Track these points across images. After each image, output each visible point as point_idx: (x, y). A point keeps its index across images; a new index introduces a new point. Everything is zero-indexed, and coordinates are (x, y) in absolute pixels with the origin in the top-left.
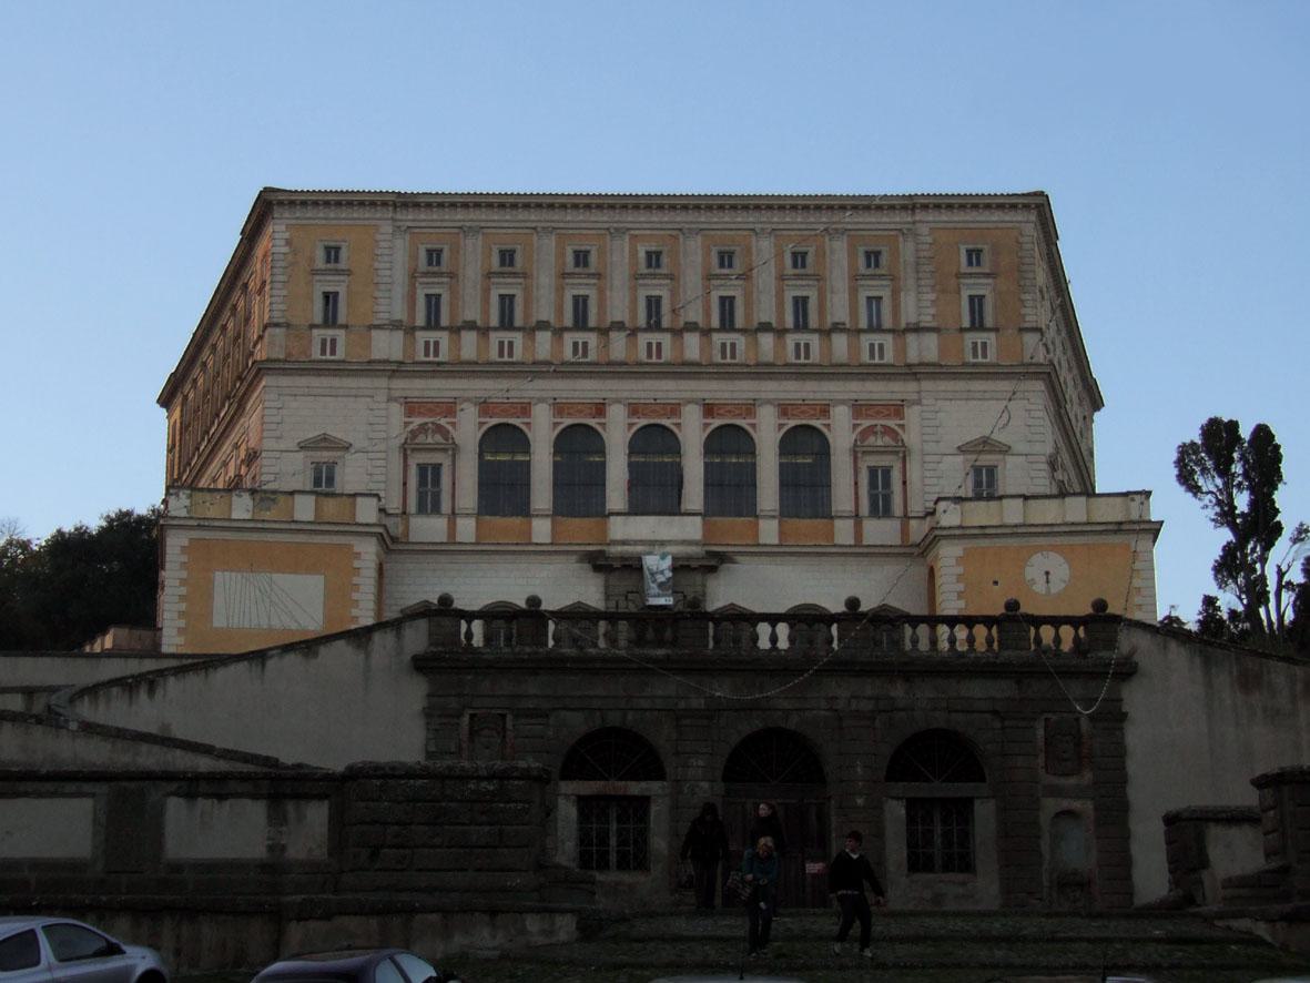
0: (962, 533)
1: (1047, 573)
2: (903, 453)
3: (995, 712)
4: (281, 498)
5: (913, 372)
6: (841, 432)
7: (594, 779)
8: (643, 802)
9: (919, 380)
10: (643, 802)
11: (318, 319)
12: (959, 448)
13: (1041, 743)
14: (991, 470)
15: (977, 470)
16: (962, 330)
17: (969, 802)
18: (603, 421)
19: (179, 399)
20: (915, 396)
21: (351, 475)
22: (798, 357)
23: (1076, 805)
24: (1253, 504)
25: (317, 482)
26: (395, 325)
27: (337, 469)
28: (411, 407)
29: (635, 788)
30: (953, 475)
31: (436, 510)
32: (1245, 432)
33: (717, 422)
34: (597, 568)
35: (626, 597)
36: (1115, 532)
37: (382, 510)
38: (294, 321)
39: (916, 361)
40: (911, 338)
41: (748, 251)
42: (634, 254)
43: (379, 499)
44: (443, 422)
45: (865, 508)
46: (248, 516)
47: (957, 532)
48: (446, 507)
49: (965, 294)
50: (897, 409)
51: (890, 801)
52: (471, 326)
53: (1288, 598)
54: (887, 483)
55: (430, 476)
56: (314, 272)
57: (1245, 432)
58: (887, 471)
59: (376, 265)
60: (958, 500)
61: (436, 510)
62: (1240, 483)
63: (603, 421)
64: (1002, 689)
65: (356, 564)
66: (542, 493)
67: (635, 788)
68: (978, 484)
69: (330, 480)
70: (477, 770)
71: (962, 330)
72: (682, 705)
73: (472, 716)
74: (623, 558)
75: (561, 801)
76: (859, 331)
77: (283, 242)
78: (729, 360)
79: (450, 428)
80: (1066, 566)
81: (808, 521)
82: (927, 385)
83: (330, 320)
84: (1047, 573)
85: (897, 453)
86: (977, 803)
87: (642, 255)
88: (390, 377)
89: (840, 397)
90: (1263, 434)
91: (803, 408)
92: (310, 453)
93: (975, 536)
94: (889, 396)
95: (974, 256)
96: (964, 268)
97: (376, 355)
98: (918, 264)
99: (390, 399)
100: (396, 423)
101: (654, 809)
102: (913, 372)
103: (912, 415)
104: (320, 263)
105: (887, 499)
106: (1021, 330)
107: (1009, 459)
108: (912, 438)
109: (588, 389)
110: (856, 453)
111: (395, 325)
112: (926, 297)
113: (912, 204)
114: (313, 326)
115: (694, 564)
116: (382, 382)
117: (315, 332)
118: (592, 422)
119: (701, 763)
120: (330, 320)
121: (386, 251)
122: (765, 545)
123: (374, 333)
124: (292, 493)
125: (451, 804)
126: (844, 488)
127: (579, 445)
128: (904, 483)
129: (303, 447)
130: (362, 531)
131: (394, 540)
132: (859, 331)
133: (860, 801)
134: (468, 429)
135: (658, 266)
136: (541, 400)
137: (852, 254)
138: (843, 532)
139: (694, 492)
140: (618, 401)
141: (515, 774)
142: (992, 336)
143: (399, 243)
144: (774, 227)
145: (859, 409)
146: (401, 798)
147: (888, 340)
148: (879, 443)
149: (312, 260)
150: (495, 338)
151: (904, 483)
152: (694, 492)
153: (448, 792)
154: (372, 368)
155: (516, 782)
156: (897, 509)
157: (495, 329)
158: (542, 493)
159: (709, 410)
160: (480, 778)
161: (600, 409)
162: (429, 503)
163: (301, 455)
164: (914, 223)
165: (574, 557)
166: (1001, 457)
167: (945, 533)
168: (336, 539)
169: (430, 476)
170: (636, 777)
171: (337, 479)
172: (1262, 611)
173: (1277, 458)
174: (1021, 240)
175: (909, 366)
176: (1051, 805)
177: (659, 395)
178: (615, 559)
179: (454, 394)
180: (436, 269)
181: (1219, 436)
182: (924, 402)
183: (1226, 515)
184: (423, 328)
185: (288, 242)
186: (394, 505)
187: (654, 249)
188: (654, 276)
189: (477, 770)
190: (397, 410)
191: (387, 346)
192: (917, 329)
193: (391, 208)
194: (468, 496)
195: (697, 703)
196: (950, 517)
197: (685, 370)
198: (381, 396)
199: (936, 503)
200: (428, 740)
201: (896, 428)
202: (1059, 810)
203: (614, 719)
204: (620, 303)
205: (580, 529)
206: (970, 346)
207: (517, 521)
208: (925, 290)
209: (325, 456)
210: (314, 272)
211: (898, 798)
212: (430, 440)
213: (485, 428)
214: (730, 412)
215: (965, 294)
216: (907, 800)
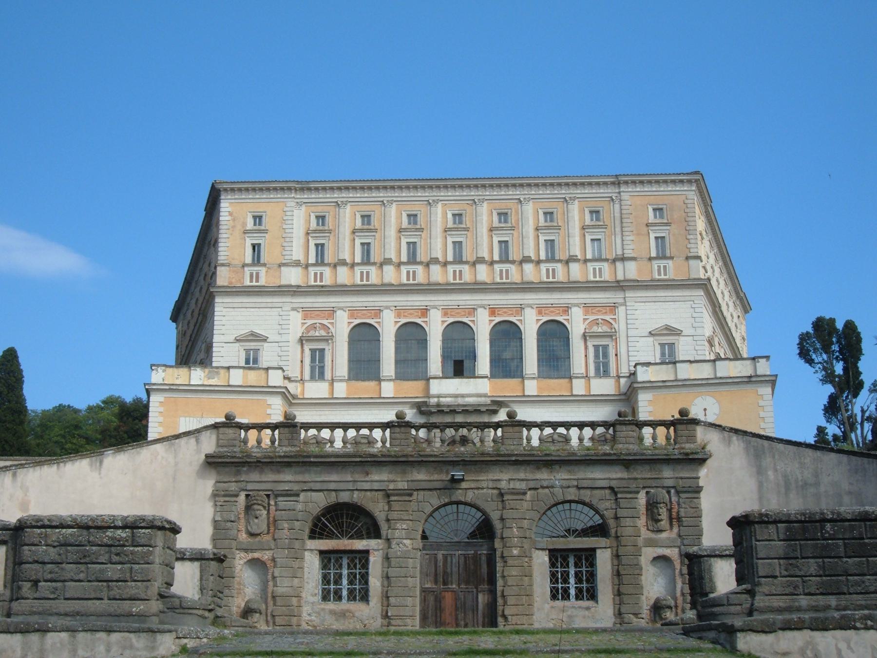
0: (651, 386)
1: (705, 410)
2: (612, 335)
3: (611, 488)
4: (222, 371)
5: (620, 286)
6: (577, 324)
7: (331, 538)
8: (365, 554)
10: (365, 554)
11: (249, 260)
13: (642, 509)
14: (672, 345)
15: (662, 345)
16: (650, 259)
17: (594, 550)
18: (425, 320)
19: (181, 316)
20: (621, 301)
21: (268, 356)
22: (548, 277)
23: (667, 552)
24: (845, 369)
25: (247, 361)
26: (297, 264)
27: (260, 353)
28: (307, 313)
29: (360, 544)
30: (648, 350)
31: (322, 376)
32: (840, 325)
33: (498, 319)
36: (747, 382)
37: (285, 378)
38: (233, 262)
39: (622, 279)
40: (619, 265)
41: (517, 213)
42: (445, 215)
43: (284, 371)
44: (325, 322)
45: (592, 372)
46: (200, 383)
47: (648, 385)
48: (328, 375)
49: (652, 236)
50: (613, 308)
51: (537, 551)
52: (343, 263)
53: (868, 426)
54: (606, 355)
55: (318, 356)
56: (246, 232)
57: (840, 325)
58: (605, 347)
59: (285, 227)
60: (648, 364)
61: (322, 376)
62: (837, 357)
63: (425, 320)
64: (616, 474)
66: (388, 366)
67: (360, 544)
68: (663, 354)
69: (256, 361)
70: (113, 522)
71: (650, 259)
72: (391, 486)
73: (247, 496)
75: (307, 554)
76: (586, 261)
77: (227, 214)
78: (504, 280)
79: (329, 326)
80: (717, 405)
81: (556, 381)
82: (629, 294)
83: (257, 260)
84: (705, 410)
85: (611, 336)
86: (598, 552)
87: (450, 216)
89: (576, 301)
90: (850, 326)
91: (552, 309)
92: (242, 344)
93: (660, 387)
94: (605, 301)
95: (658, 210)
96: (651, 219)
97: (284, 282)
98: (621, 218)
99: (294, 309)
100: (296, 325)
101: (372, 559)
102: (620, 286)
103: (621, 310)
104: (250, 225)
105: (606, 365)
106: (687, 258)
107: (682, 338)
108: (621, 327)
109: (418, 300)
110: (585, 337)
111: (297, 264)
112: (628, 238)
114: (244, 266)
115: (483, 409)
117: (246, 269)
118: (419, 321)
119: (404, 526)
120: (257, 260)
121: (290, 218)
122: (529, 396)
123: (284, 269)
124: (228, 368)
125: (94, 548)
126: (580, 357)
127: (412, 336)
128: (616, 355)
129: (237, 340)
130: (273, 391)
131: (294, 397)
132: (586, 261)
133: (515, 552)
134: (342, 326)
135: (461, 223)
136: (387, 308)
137: (582, 211)
138: (579, 387)
139: (483, 364)
140: (435, 307)
141: (142, 525)
142: (670, 262)
143: (296, 212)
144: (532, 197)
145: (588, 308)
146: (56, 544)
147: (605, 266)
148: (600, 330)
150: (358, 270)
151: (616, 355)
152: (483, 364)
153: (91, 539)
155: (143, 531)
156: (613, 372)
157: (358, 264)
158: (388, 366)
159: (493, 312)
160: (116, 528)
161: (424, 312)
162: (318, 372)
163: (237, 345)
164: (619, 193)
166: (677, 337)
167: (640, 385)
169: (318, 356)
170: (359, 536)
171: (260, 359)
172: (853, 436)
173: (859, 340)
174: (686, 201)
175: (618, 282)
176: (648, 553)
177: (461, 303)
178: (433, 406)
179: (333, 305)
180: (321, 228)
181: (823, 328)
182: (628, 304)
183: (829, 377)
184: (313, 265)
185: (231, 214)
186: (295, 373)
187: (456, 212)
188: (457, 229)
189: (113, 522)
191: (292, 276)
192: (623, 259)
194: (343, 369)
195: (402, 485)
196: (643, 375)
197: (478, 288)
198: (287, 307)
199: (635, 366)
200: (215, 512)
201: (611, 321)
202: (655, 555)
203: (344, 497)
204: (437, 245)
205: (413, 389)
206: (656, 268)
207: (372, 384)
208: (627, 233)
209: (252, 345)
210: (246, 232)
211: (543, 549)
212: (317, 334)
213: (352, 325)
214: (505, 312)
215: (652, 236)
216: (550, 551)
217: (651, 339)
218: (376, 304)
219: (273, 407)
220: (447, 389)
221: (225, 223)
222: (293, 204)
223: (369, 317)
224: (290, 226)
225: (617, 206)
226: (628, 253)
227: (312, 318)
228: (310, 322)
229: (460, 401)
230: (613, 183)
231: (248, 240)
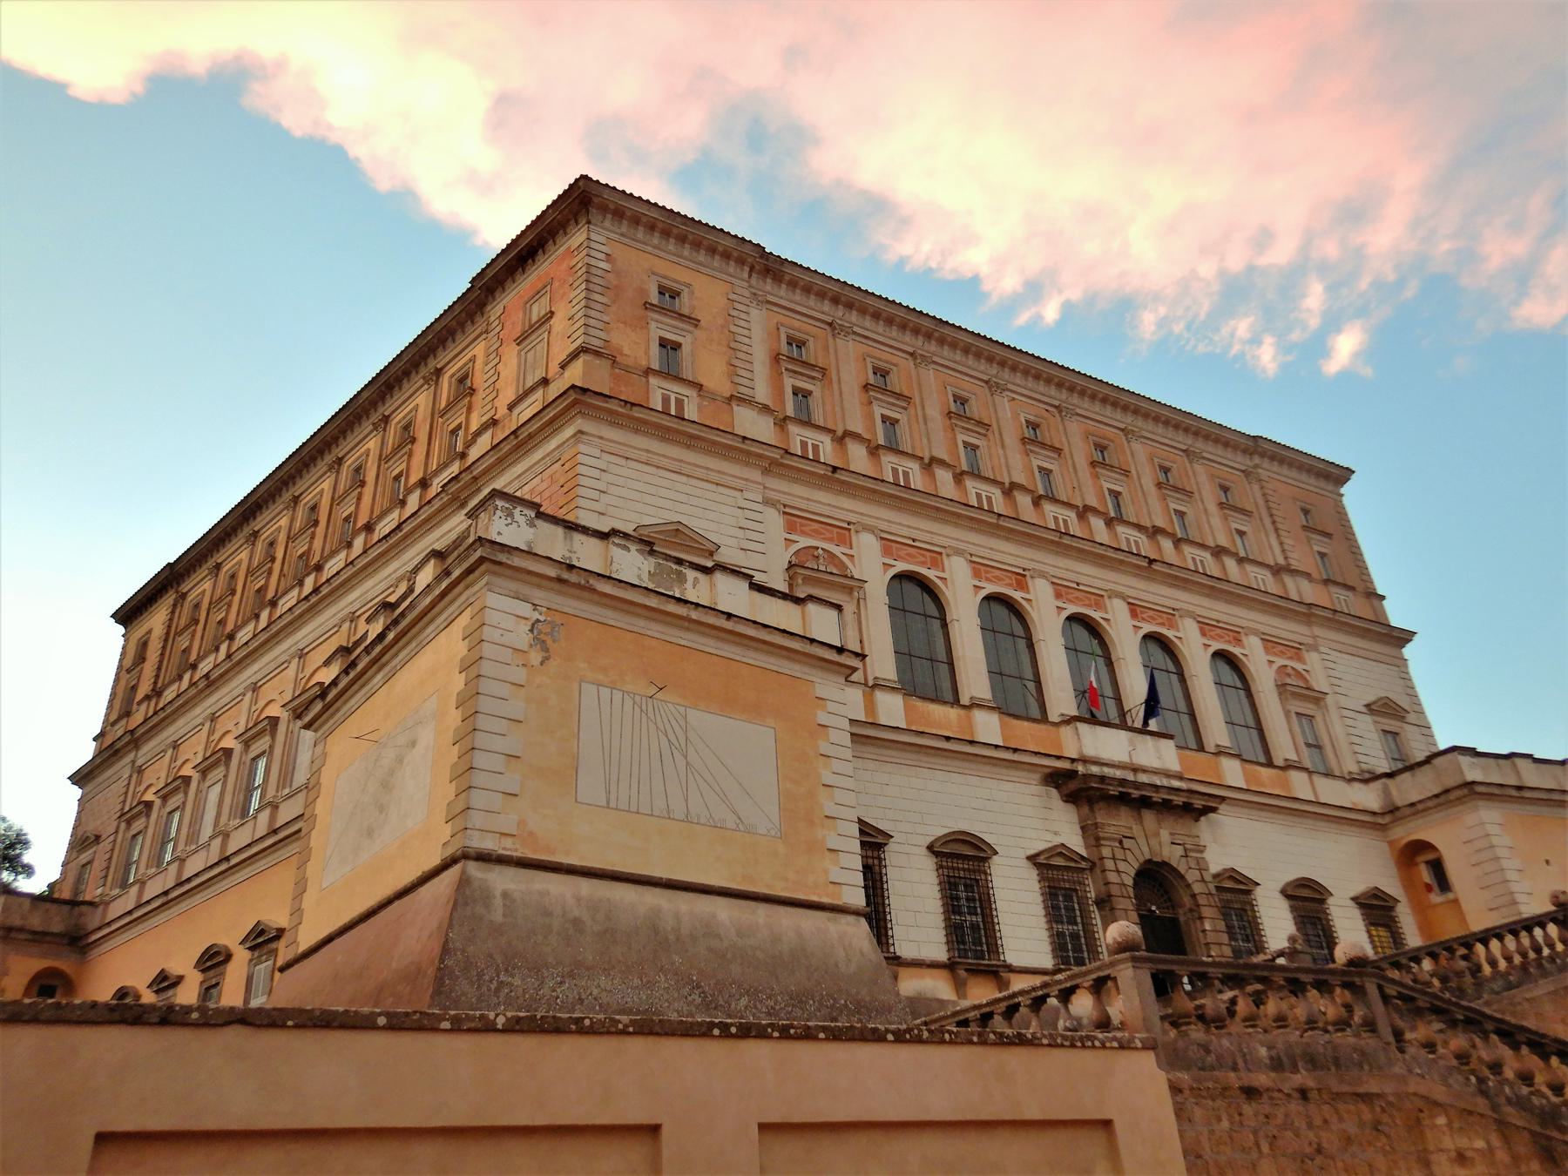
9: (1309, 623)
12: (1367, 706)
28: (794, 520)
34: (1072, 798)
35: (1121, 842)
59: (733, 328)
65: (823, 718)
74: (1123, 782)
88: (766, 472)
99: (767, 502)
103: (1312, 658)
104: (654, 298)
113: (1257, 447)
116: (756, 475)
149: (642, 291)
154: (741, 450)
165: (1037, 776)
168: (796, 669)
187: (1032, 418)
190: (774, 521)
193: (747, 269)
217: (1368, 719)
218: (936, 540)
219: (831, 707)
220: (1108, 747)
221: (599, 272)
222: (747, 293)
223: (923, 564)
224: (746, 332)
225: (1256, 487)
226: (1295, 564)
227: (815, 534)
228: (804, 542)
229: (1143, 778)
230: (1245, 451)
231: (653, 325)
